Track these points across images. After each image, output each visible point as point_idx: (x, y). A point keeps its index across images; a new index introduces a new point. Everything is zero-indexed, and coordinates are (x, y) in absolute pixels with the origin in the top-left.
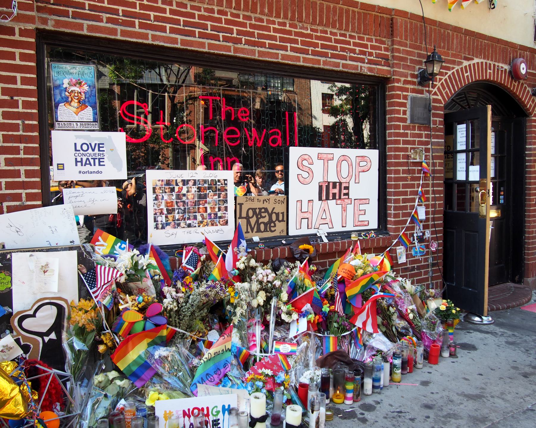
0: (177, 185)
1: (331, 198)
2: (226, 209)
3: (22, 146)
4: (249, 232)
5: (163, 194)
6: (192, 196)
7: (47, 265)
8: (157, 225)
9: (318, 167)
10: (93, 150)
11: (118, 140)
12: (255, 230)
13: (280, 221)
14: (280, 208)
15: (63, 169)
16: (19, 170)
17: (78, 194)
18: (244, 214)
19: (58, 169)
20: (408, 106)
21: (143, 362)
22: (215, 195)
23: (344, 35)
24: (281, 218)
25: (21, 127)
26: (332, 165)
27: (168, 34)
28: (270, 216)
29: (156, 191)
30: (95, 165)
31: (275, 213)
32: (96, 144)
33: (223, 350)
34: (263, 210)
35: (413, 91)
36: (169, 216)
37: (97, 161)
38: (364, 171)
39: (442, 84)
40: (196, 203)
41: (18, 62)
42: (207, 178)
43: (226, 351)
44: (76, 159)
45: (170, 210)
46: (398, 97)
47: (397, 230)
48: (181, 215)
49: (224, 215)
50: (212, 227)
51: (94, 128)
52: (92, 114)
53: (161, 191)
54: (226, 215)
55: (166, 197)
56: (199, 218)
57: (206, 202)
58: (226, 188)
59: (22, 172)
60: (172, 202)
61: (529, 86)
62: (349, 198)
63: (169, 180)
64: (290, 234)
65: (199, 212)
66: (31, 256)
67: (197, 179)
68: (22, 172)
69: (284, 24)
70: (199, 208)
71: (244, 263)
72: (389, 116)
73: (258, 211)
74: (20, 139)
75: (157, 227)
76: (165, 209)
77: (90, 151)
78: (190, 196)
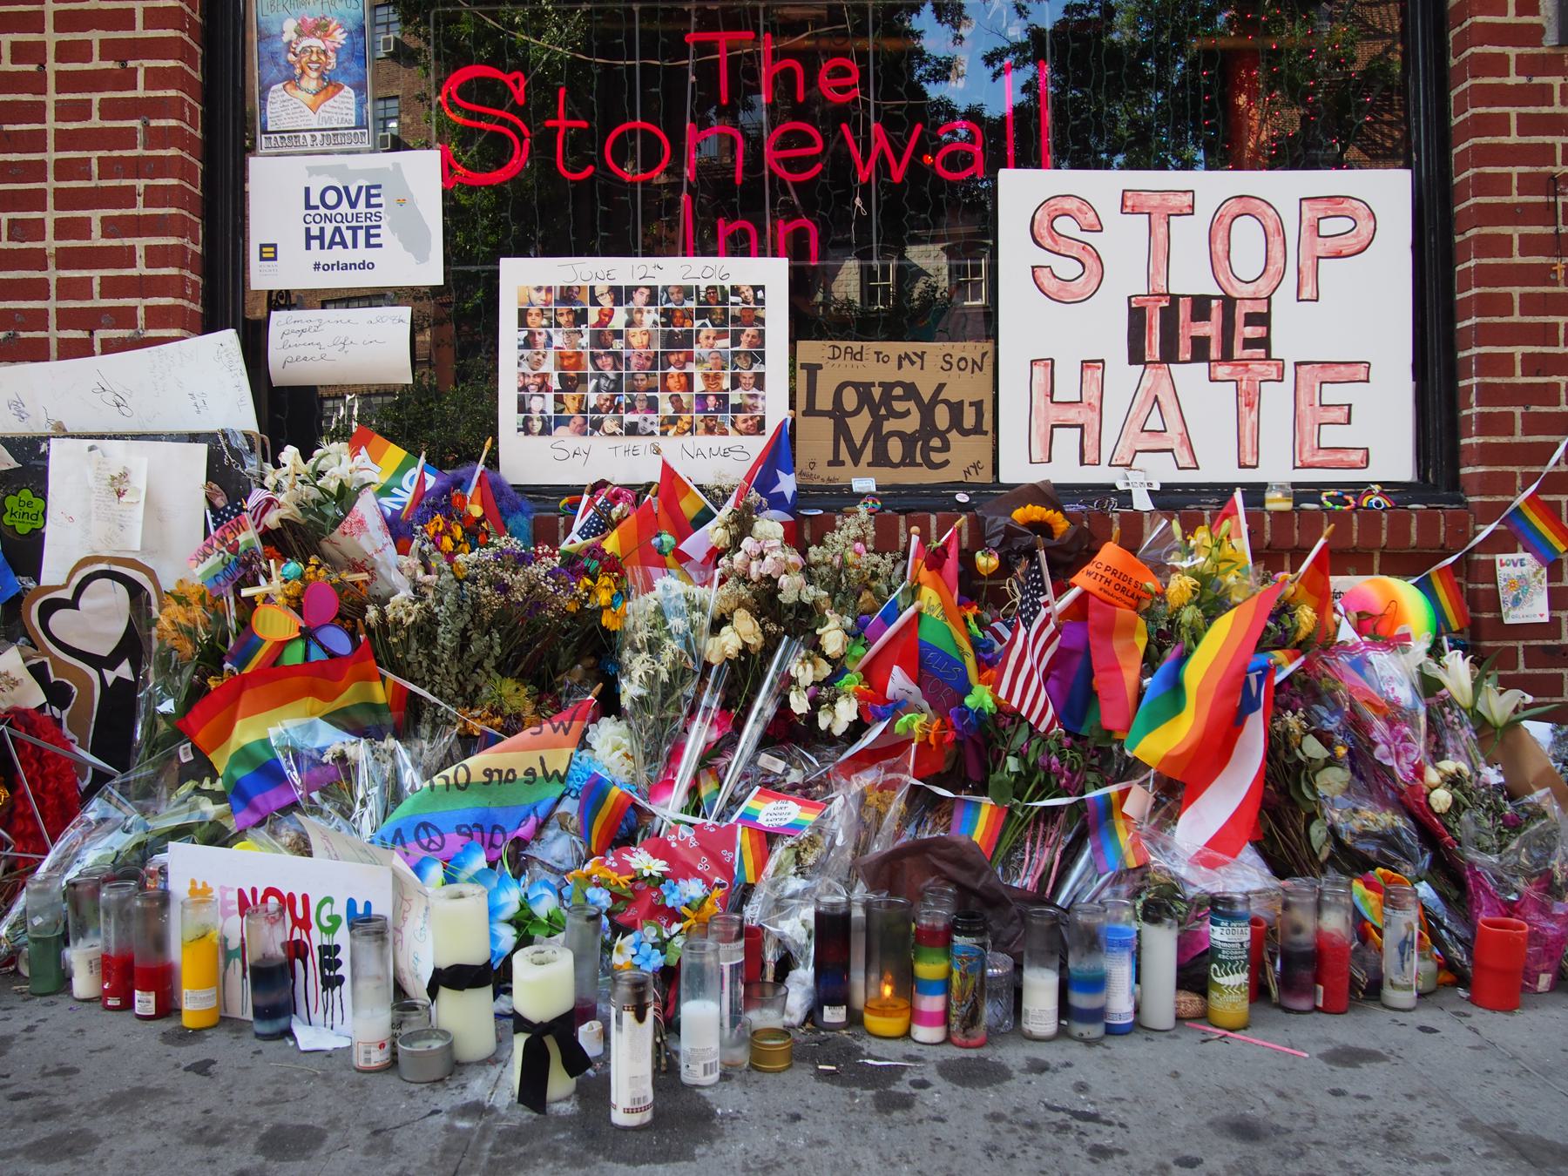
0: (594, 302)
2: (759, 381)
3: (141, 184)
4: (843, 464)
5: (552, 331)
6: (645, 338)
7: (124, 475)
8: (526, 421)
10: (353, 205)
12: (867, 455)
13: (965, 433)
14: (963, 387)
15: (275, 259)
16: (133, 248)
17: (306, 326)
18: (824, 401)
19: (262, 259)
21: (268, 757)
22: (720, 335)
24: (969, 420)
25: (140, 136)
28: (927, 411)
29: (529, 319)
30: (355, 246)
31: (946, 402)
32: (360, 188)
33: (530, 772)
34: (898, 391)
36: (567, 396)
37: (361, 234)
38: (1339, 255)
40: (654, 361)
42: (693, 283)
43: (548, 778)
44: (308, 230)
45: (572, 379)
47: (1506, 484)
48: (606, 395)
49: (750, 402)
50: (710, 437)
51: (359, 146)
52: (353, 107)
53: (545, 322)
54: (760, 403)
55: (558, 340)
56: (666, 408)
57: (689, 358)
58: (760, 313)
59: (140, 252)
60: (579, 354)
62: (1268, 357)
63: (570, 288)
64: (1003, 479)
65: (665, 389)
66: (91, 449)
67: (659, 283)
68: (140, 252)
70: (665, 377)
71: (726, 526)
72: (1458, 29)
73: (877, 392)
74: (136, 168)
75: (526, 429)
76: (555, 375)
77: (345, 207)
78: (637, 337)
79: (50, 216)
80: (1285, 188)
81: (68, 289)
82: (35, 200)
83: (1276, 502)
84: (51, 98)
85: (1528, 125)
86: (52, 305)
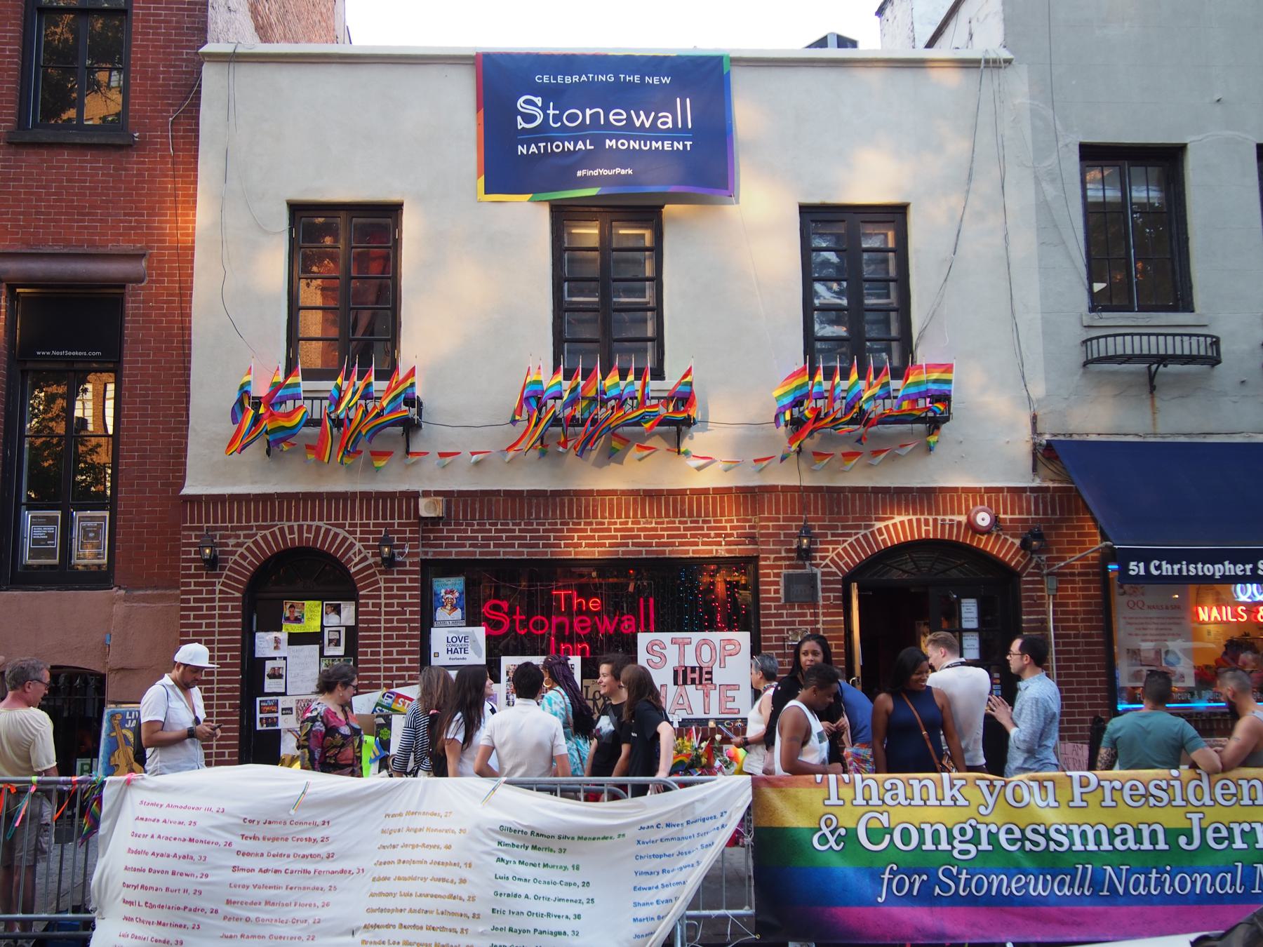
1: (689, 681)
9: (672, 653)
11: (480, 633)
20: (782, 584)
23: (697, 522)
26: (690, 650)
27: (516, 549)
35: (788, 567)
39: (838, 555)
41: (408, 584)
46: (768, 575)
61: (1013, 536)
69: (627, 523)
74: (406, 637)
79: (382, 650)
80: (716, 637)
81: (386, 669)
82: (378, 645)
83: (712, 724)
84: (383, 617)
85: (777, 623)
86: (382, 674)
